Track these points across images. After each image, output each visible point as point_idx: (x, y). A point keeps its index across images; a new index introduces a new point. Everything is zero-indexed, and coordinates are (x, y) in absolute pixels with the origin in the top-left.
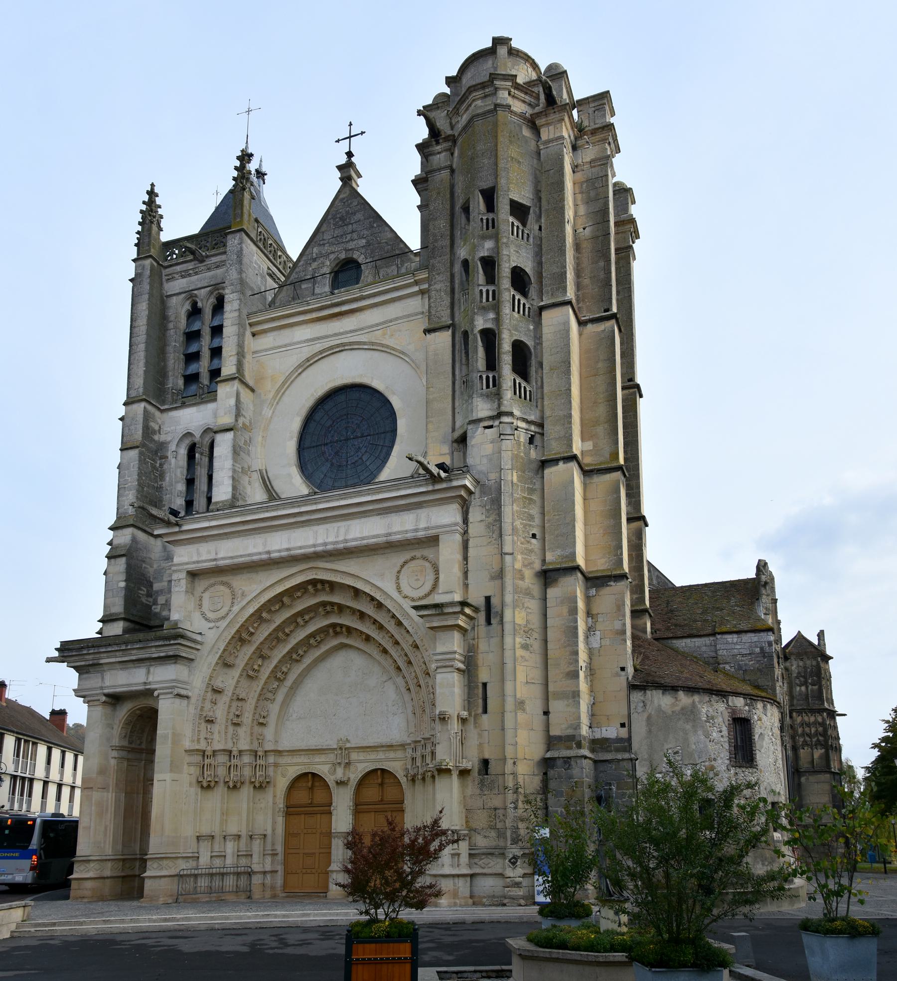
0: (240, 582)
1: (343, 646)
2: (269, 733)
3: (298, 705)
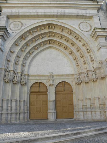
0: (25, 21)
1: (50, 47)
2: (26, 69)
3: (35, 62)
